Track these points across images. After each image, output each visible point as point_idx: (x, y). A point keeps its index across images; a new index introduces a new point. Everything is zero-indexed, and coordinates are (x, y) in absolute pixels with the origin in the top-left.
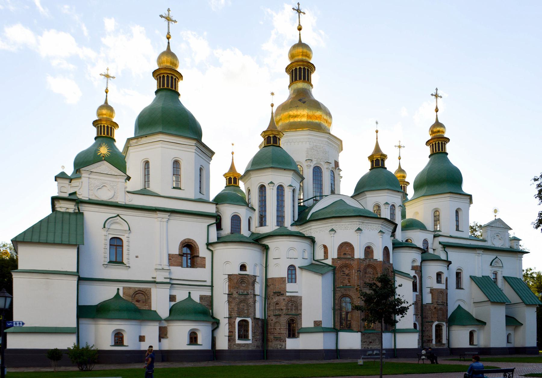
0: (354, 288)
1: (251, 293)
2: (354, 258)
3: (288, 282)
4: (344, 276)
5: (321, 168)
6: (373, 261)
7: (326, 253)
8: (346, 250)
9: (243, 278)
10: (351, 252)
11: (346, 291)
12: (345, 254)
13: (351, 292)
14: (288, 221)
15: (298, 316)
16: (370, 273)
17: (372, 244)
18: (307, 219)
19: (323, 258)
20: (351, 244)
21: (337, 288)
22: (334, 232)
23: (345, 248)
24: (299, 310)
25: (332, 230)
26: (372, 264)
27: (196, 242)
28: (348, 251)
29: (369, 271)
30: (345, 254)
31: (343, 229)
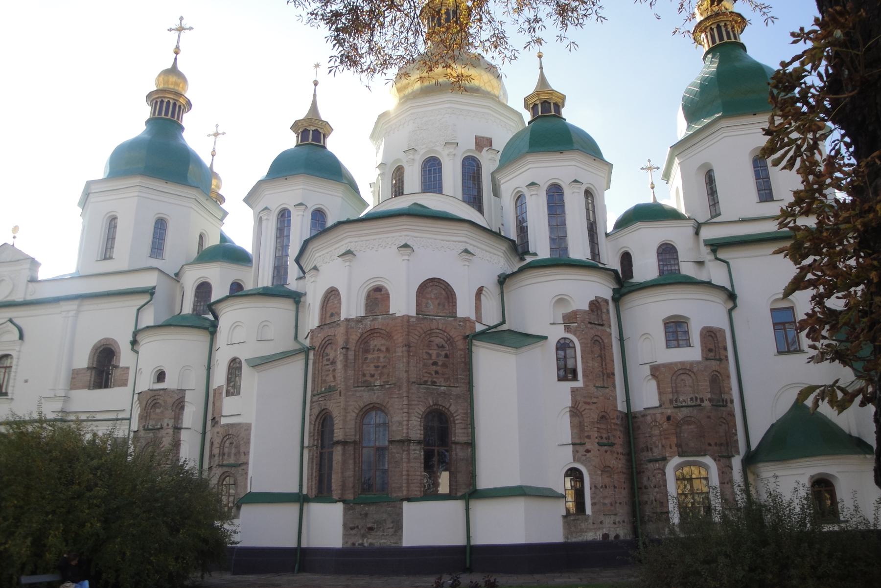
0: (337, 390)
1: (168, 425)
3: (227, 396)
4: (328, 365)
6: (382, 319)
9: (156, 397)
11: (325, 402)
12: (332, 315)
13: (332, 401)
15: (240, 469)
16: (379, 350)
21: (315, 395)
24: (243, 454)
26: (380, 327)
27: (116, 342)
29: (376, 346)
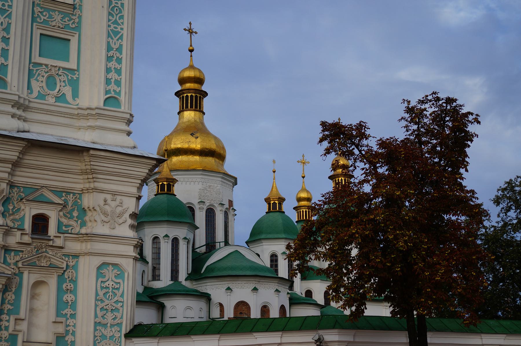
2: (251, 318)
5: (214, 210)
7: (222, 311)
8: (242, 309)
10: (248, 311)
12: (241, 313)
14: (182, 276)
17: (269, 304)
18: (202, 272)
19: (219, 317)
20: (247, 303)
22: (231, 290)
23: (242, 307)
25: (229, 289)
28: (244, 310)
30: (241, 313)
31: (239, 287)
